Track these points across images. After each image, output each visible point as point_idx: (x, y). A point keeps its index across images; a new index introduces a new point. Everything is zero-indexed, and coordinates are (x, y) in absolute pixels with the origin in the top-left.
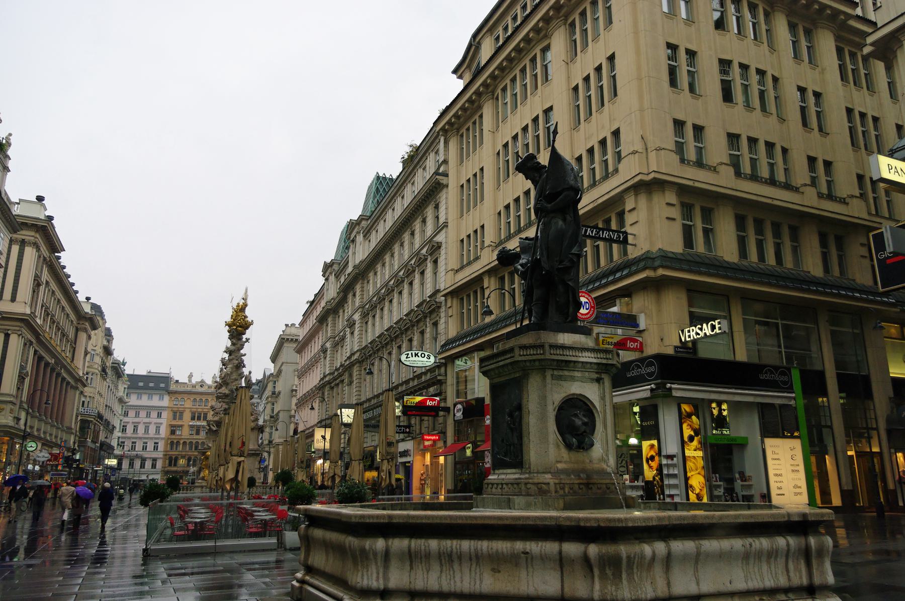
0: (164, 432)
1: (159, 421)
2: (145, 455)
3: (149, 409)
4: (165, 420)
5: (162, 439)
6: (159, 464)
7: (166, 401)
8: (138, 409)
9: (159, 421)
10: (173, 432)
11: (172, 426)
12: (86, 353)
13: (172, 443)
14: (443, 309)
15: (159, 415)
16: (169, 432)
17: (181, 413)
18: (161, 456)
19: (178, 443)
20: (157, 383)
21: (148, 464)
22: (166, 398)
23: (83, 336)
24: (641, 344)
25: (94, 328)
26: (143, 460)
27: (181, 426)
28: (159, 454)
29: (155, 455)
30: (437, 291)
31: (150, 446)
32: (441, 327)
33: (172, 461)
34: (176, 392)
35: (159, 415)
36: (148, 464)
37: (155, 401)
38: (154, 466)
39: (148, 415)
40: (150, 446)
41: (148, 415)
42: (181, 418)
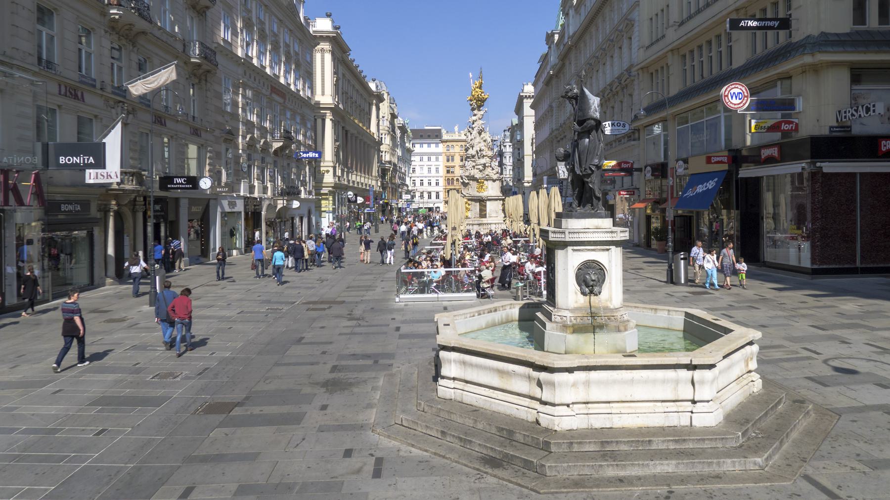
0: (442, 171)
1: (437, 163)
2: (430, 189)
3: (429, 155)
4: (442, 162)
7: (441, 148)
8: (421, 155)
9: (437, 163)
10: (448, 172)
11: (447, 167)
14: (636, 82)
17: (453, 157)
22: (441, 145)
24: (797, 125)
27: (453, 167)
28: (440, 189)
30: (632, 66)
32: (635, 98)
34: (446, 141)
35: (437, 159)
37: (433, 148)
38: (438, 197)
39: (429, 159)
41: (429, 159)
42: (453, 160)
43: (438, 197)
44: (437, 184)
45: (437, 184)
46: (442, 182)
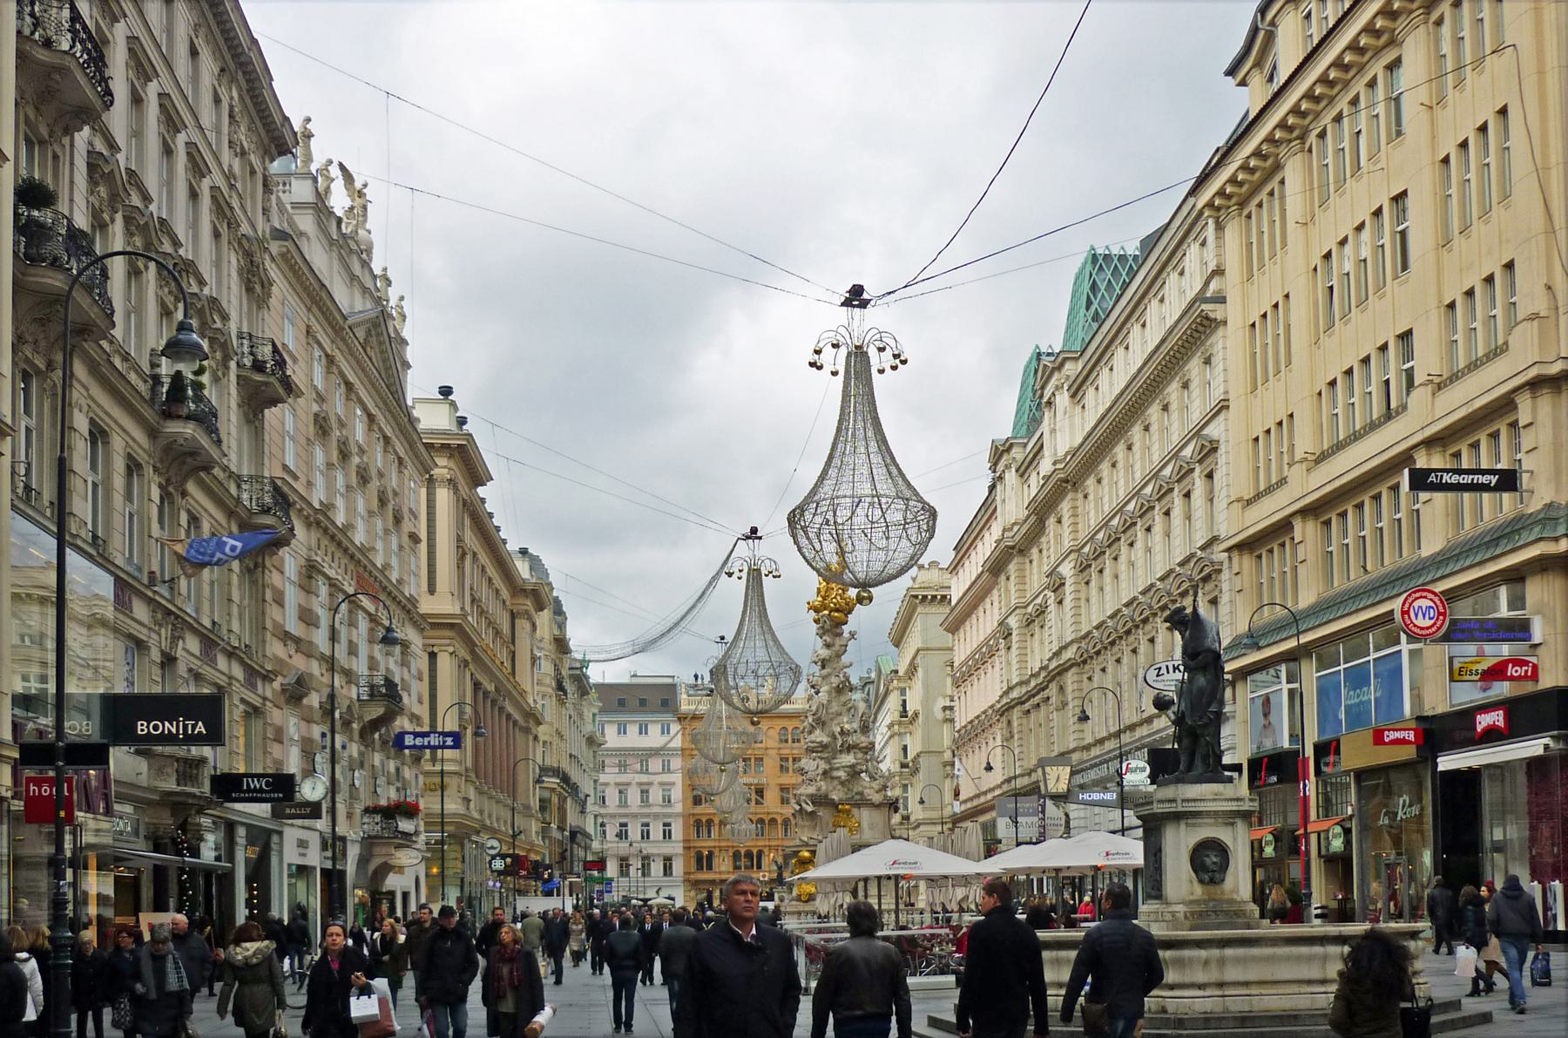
1: (666, 778)
2: (648, 849)
5: (677, 815)
6: (678, 867)
8: (625, 757)
9: (666, 778)
10: (697, 801)
12: (534, 659)
13: (698, 824)
15: (667, 769)
16: (690, 801)
18: (680, 851)
19: (710, 822)
20: (653, 699)
21: (657, 868)
23: (523, 625)
25: (540, 608)
26: (646, 860)
28: (675, 848)
29: (667, 849)
31: (656, 831)
33: (703, 861)
36: (657, 868)
38: (667, 871)
40: (656, 831)
43: (667, 871)
44: (667, 835)
45: (667, 835)
46: (677, 831)
